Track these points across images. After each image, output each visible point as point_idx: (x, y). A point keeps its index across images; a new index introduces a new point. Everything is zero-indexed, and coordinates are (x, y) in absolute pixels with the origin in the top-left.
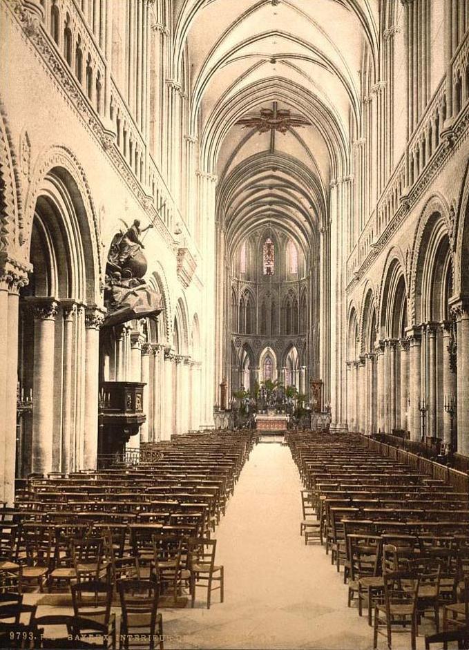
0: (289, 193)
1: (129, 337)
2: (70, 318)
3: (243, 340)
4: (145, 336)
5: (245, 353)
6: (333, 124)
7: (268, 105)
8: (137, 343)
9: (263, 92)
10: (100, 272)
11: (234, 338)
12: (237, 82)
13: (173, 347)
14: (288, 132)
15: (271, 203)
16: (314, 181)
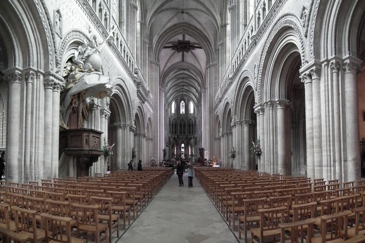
0: (190, 81)
1: (99, 111)
2: (30, 81)
3: (173, 136)
4: (110, 112)
5: (174, 141)
6: (208, 42)
7: (180, 37)
8: (104, 115)
9: (178, 29)
10: (56, 53)
11: (170, 136)
12: (167, 24)
13: (134, 126)
14: (189, 52)
15: (183, 86)
16: (200, 73)
